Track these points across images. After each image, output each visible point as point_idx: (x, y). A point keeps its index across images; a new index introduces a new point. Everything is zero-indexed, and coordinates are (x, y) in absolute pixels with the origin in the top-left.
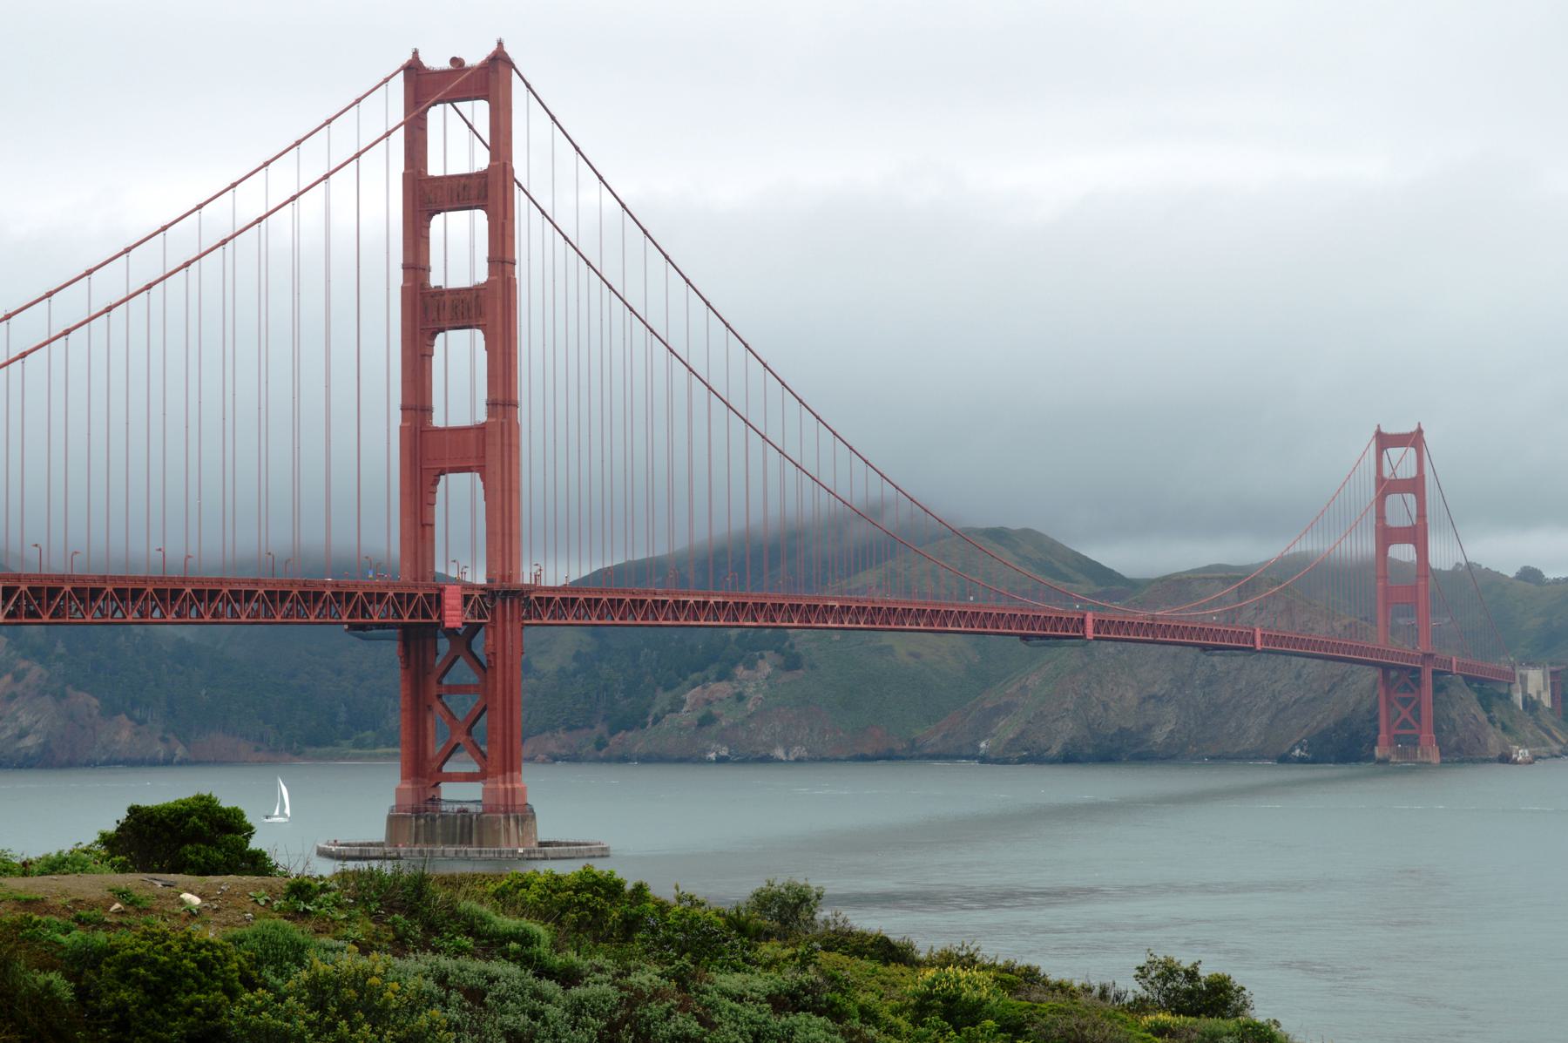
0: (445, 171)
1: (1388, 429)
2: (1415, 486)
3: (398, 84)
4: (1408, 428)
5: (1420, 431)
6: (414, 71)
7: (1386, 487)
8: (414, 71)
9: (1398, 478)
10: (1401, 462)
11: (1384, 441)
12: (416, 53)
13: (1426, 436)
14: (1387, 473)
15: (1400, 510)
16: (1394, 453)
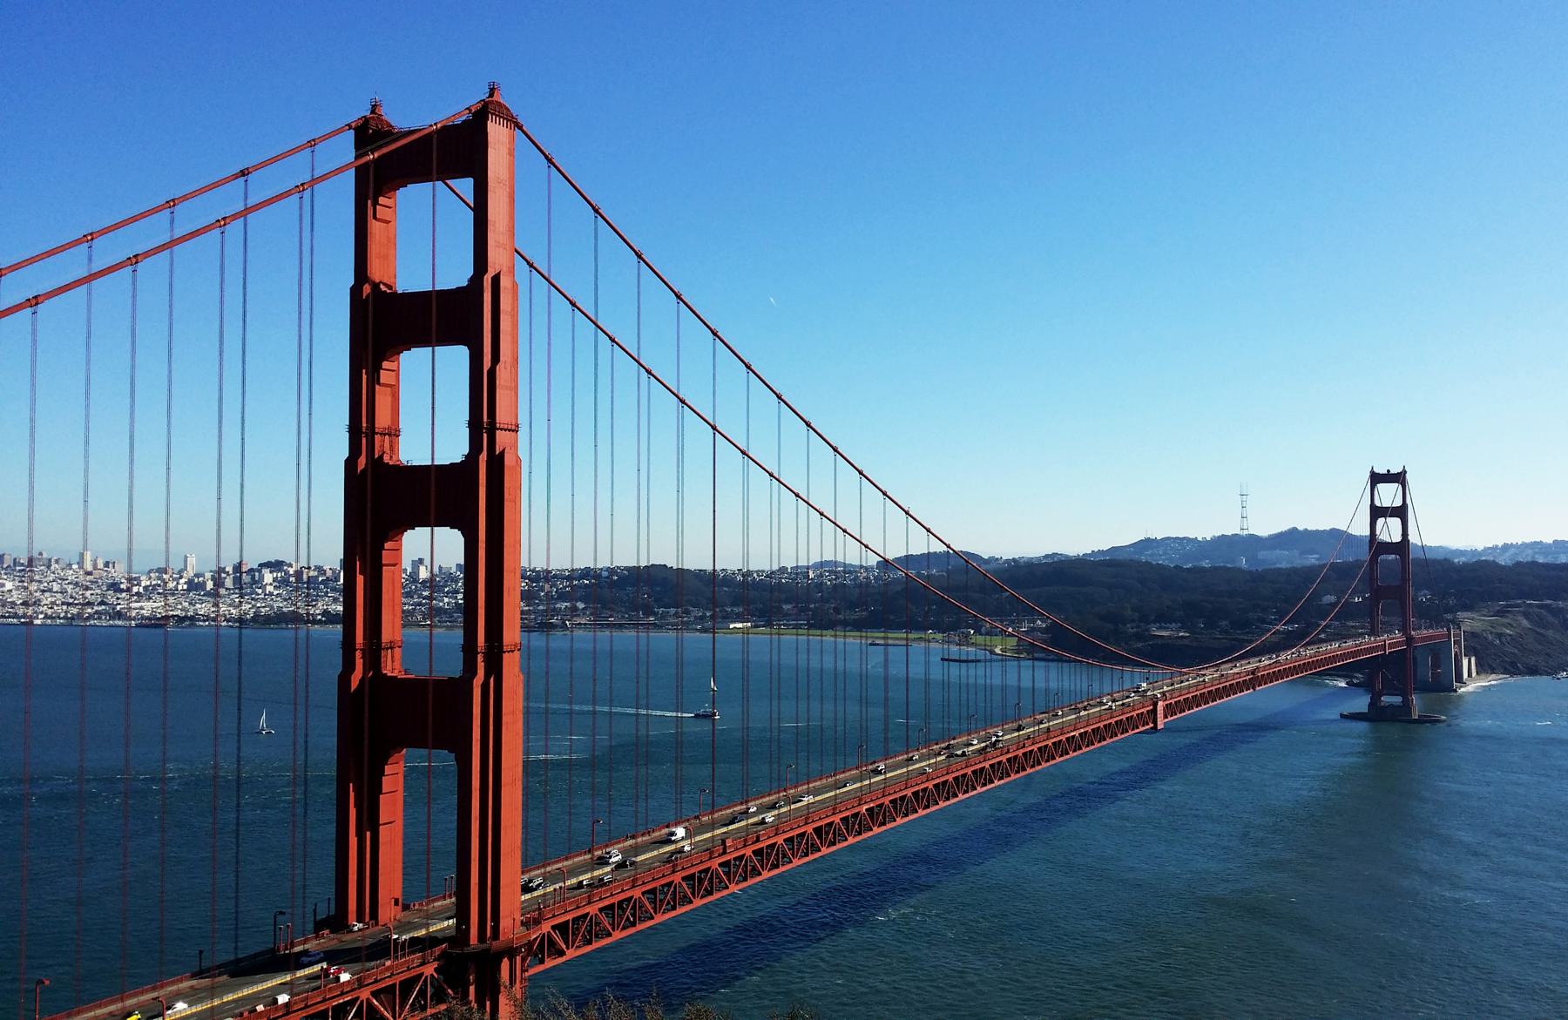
0: (433, 287)
1: (1381, 470)
2: (1401, 512)
3: (344, 150)
4: (1392, 472)
5: (1404, 472)
6: (369, 133)
7: (1377, 512)
8: (369, 133)
9: (1384, 506)
10: (1388, 495)
11: (1376, 479)
12: (374, 108)
13: (1408, 476)
14: (1378, 504)
15: (1390, 530)
16: (1380, 486)
